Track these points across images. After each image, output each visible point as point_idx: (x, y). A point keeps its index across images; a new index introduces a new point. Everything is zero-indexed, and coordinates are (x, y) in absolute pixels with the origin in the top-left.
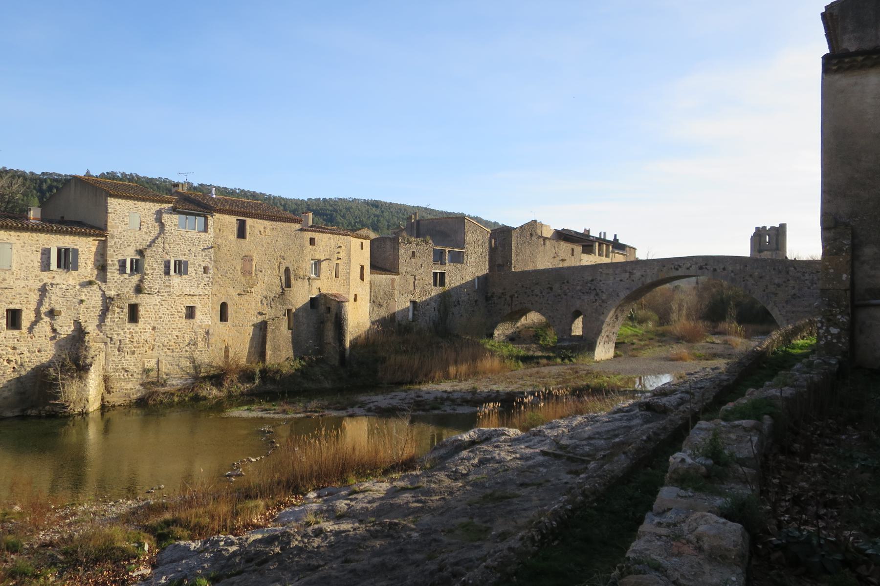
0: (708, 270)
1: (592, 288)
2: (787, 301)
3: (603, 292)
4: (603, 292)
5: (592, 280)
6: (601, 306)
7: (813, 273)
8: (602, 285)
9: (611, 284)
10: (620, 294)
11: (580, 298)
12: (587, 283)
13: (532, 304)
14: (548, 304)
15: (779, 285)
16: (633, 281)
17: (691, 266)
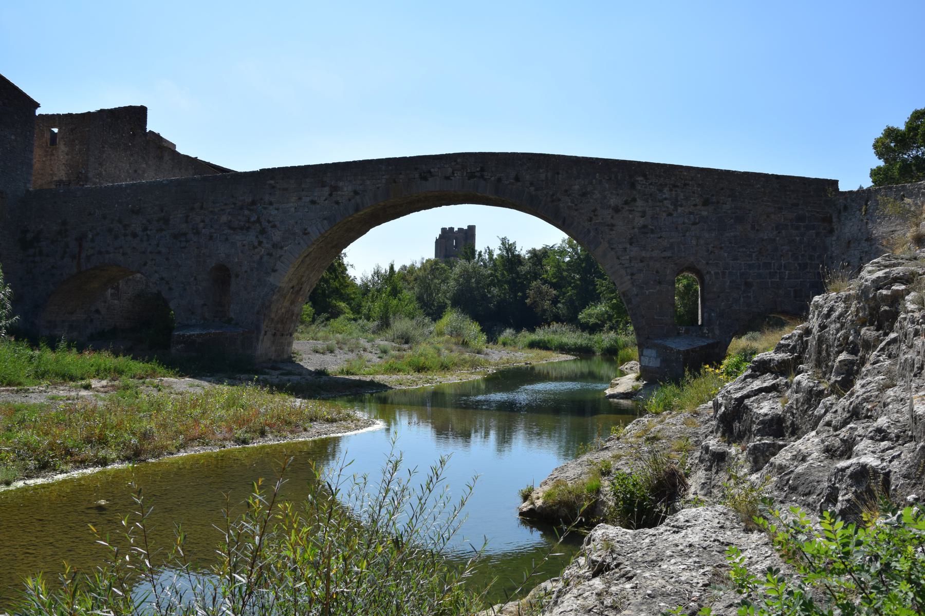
0: (485, 180)
1: (252, 219)
2: (631, 239)
3: (274, 226)
4: (274, 226)
5: (253, 203)
6: (270, 255)
7: (677, 186)
8: (274, 212)
9: (293, 209)
10: (309, 230)
11: (227, 239)
12: (241, 208)
13: (124, 254)
14: (159, 253)
15: (617, 210)
16: (337, 203)
17: (453, 173)
